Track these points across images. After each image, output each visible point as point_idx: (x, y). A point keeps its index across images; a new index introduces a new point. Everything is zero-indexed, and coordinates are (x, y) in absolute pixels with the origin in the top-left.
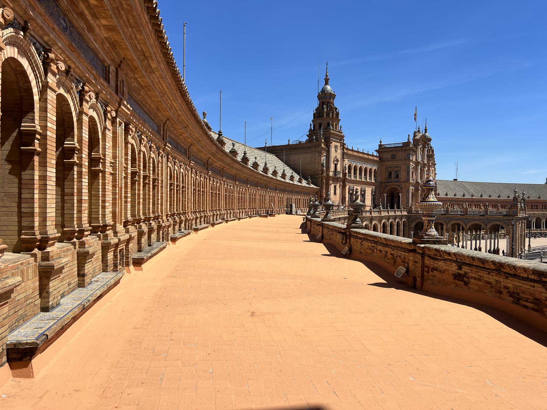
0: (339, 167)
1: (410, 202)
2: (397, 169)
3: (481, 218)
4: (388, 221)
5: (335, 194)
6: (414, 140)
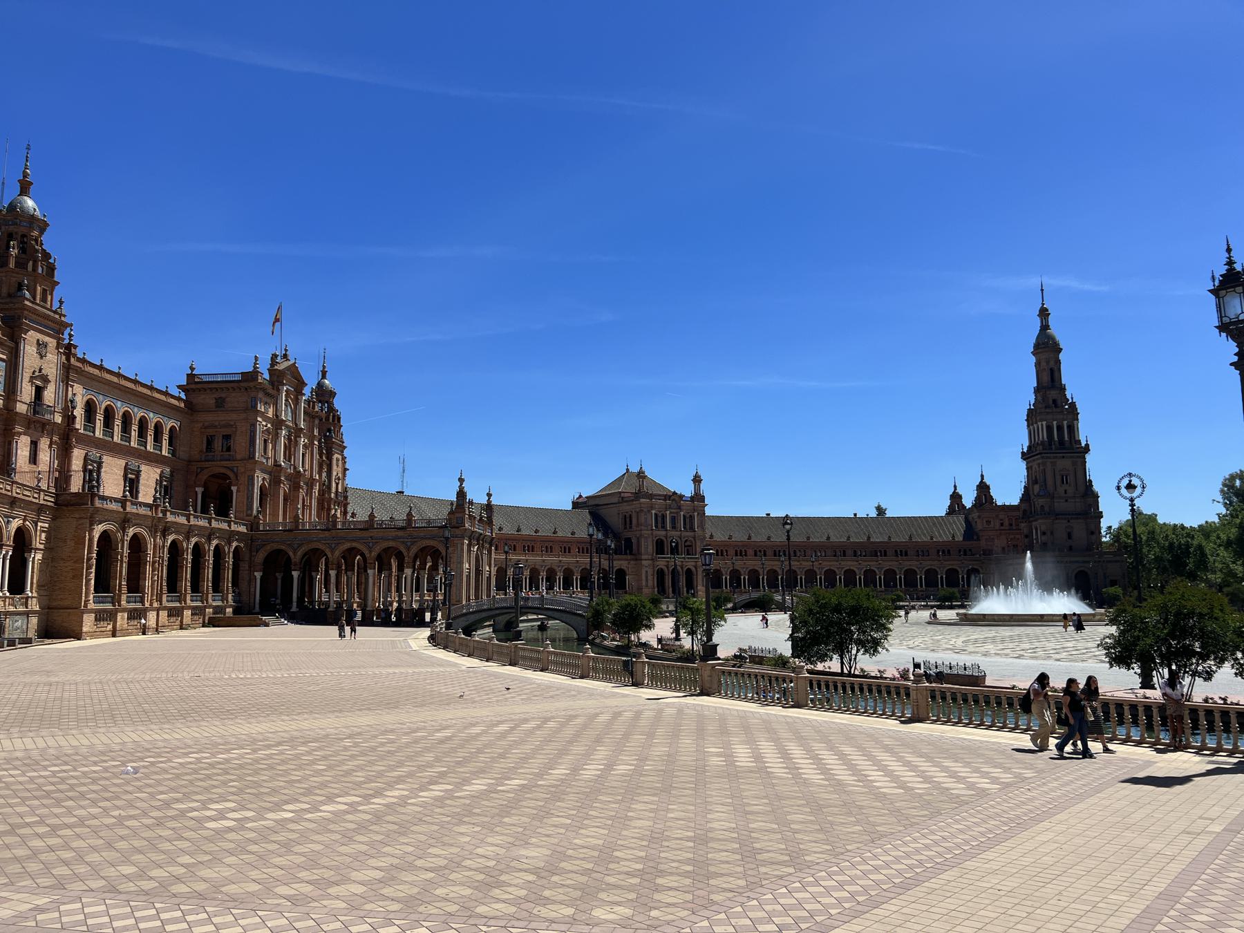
0: (49, 396)
1: (256, 504)
2: (226, 431)
3: (400, 533)
4: (188, 539)
5: (34, 459)
6: (271, 371)
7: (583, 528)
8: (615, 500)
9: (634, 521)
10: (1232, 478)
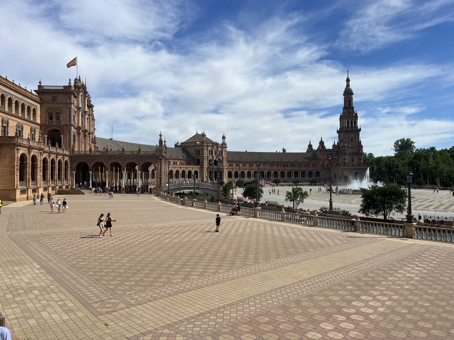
1: (72, 143)
7: (181, 155)
8: (193, 144)
9: (201, 153)
10: (398, 141)
